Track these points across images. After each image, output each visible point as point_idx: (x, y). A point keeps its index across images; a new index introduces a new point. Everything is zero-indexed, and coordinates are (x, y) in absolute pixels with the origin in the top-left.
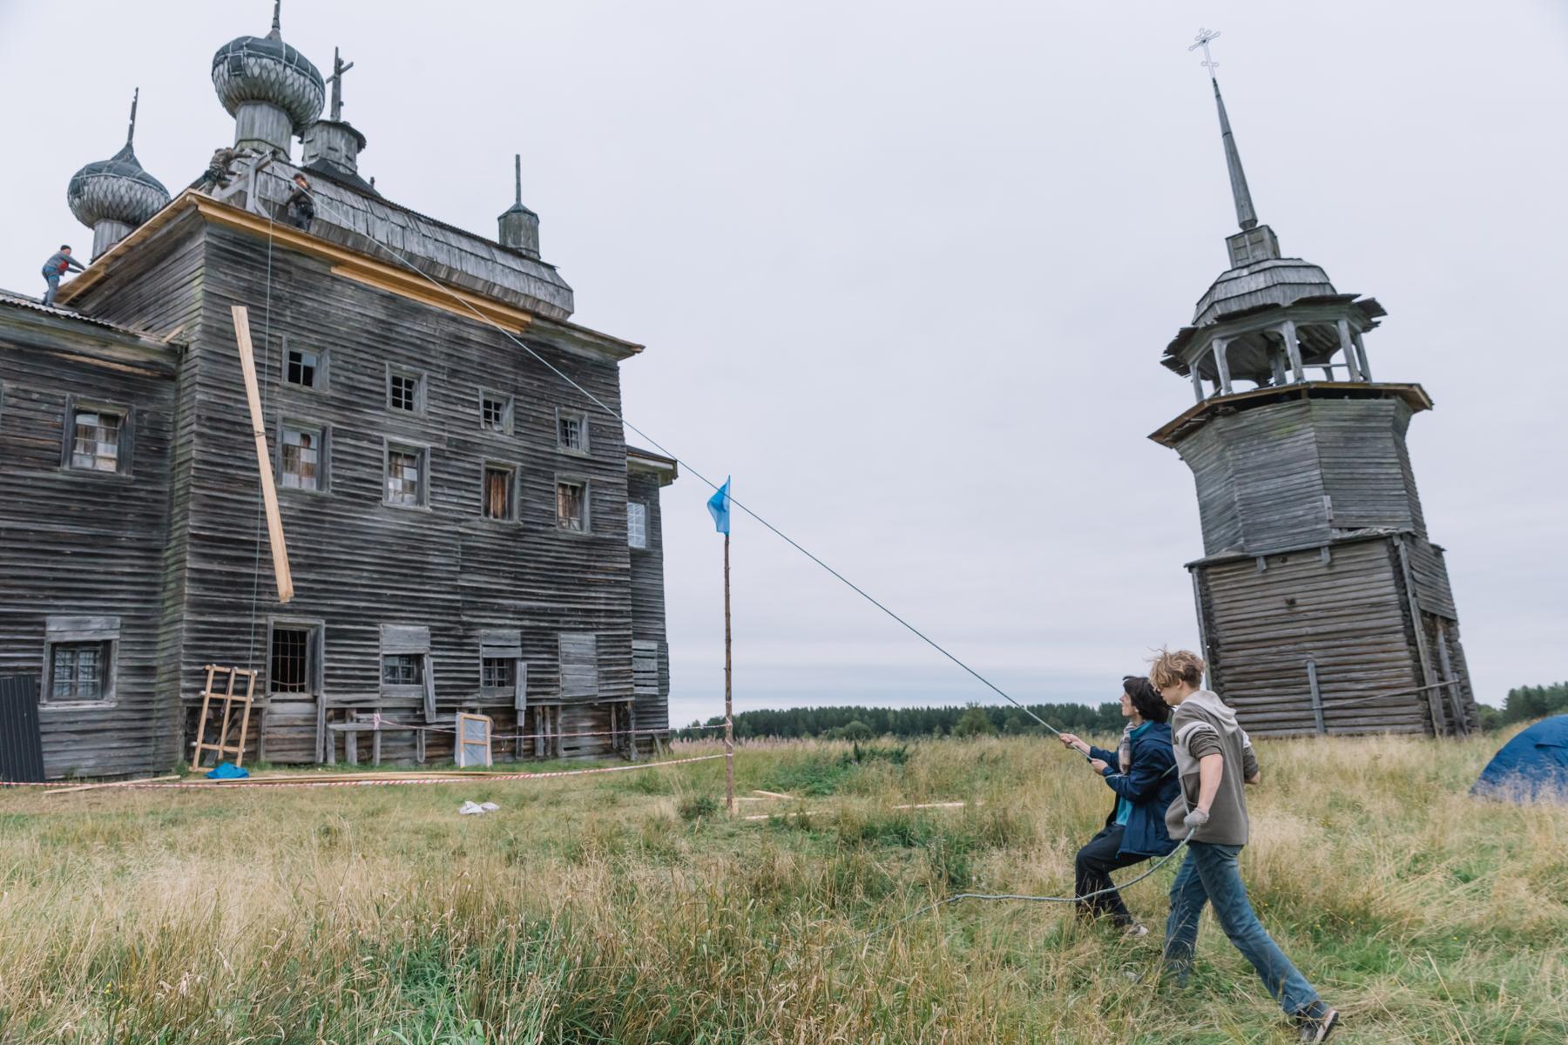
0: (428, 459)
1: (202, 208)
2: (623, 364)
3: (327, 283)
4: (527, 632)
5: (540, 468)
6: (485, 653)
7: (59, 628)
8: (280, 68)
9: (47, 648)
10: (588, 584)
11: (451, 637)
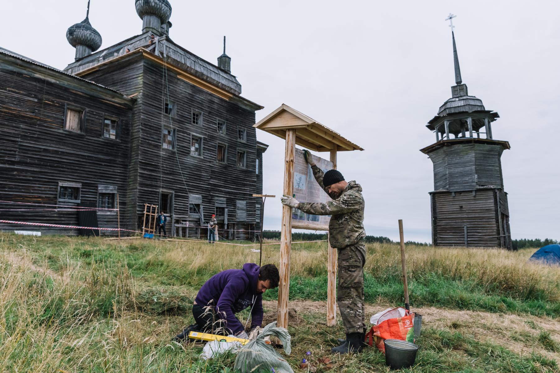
0: (202, 141)
1: (144, 54)
2: (257, 112)
3: (176, 80)
4: (228, 199)
5: (233, 146)
6: (217, 205)
7: (101, 188)
8: (161, 4)
9: (98, 194)
10: (245, 185)
11: (208, 199)
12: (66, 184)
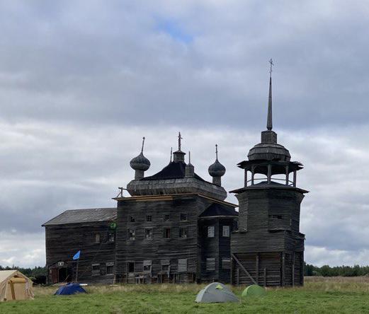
6: (163, 264)
7: (107, 264)
12: (93, 265)
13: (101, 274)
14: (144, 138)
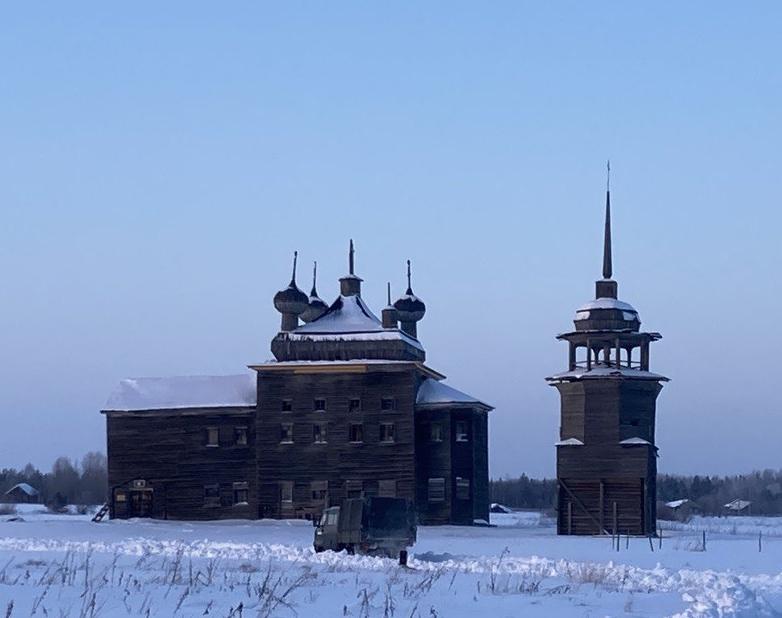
11: (336, 483)
13: (224, 504)
14: (296, 253)
